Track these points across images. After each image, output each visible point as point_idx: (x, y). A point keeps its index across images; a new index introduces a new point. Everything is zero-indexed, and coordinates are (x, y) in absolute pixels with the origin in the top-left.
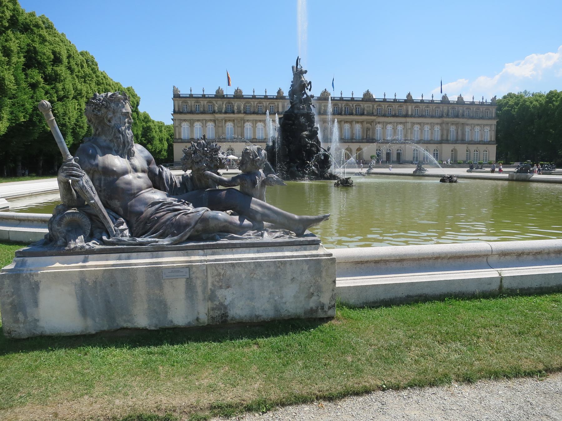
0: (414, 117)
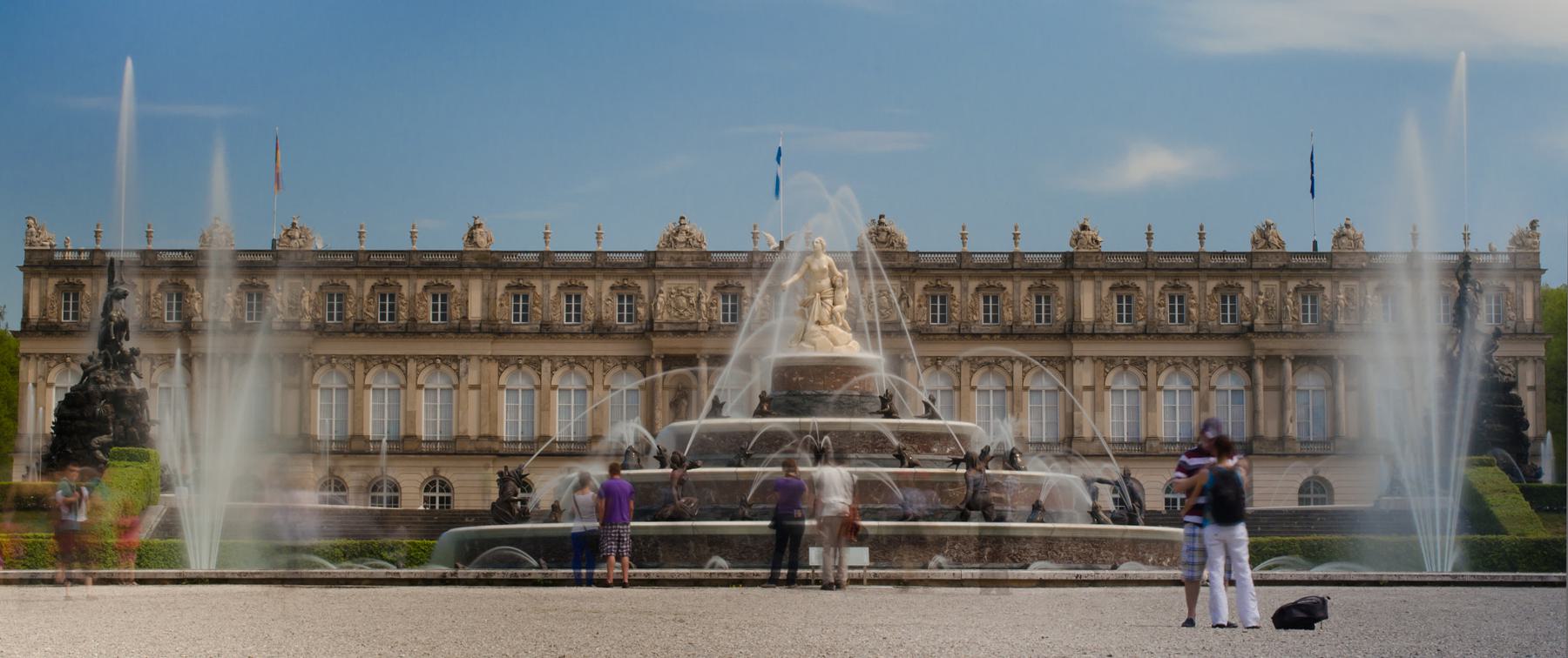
0: (1110, 336)
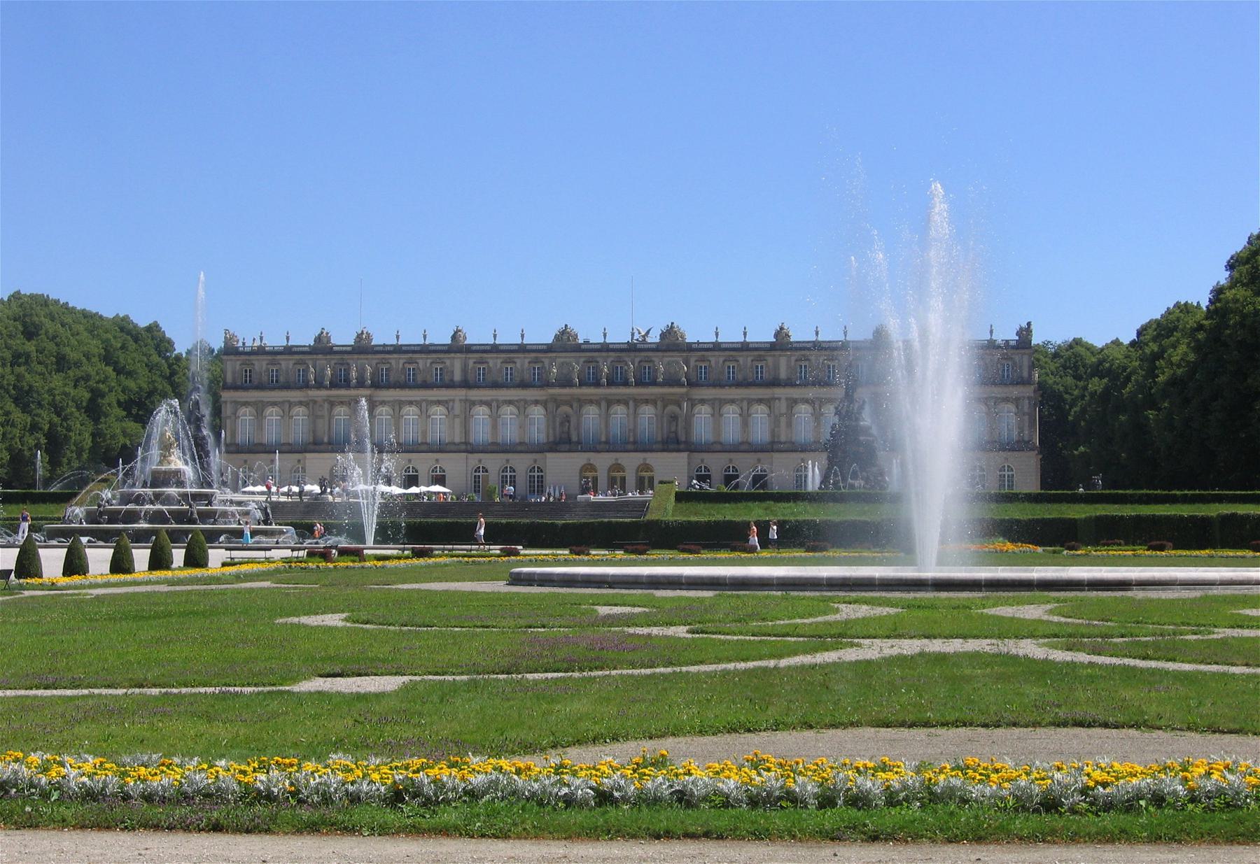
0: (793, 385)
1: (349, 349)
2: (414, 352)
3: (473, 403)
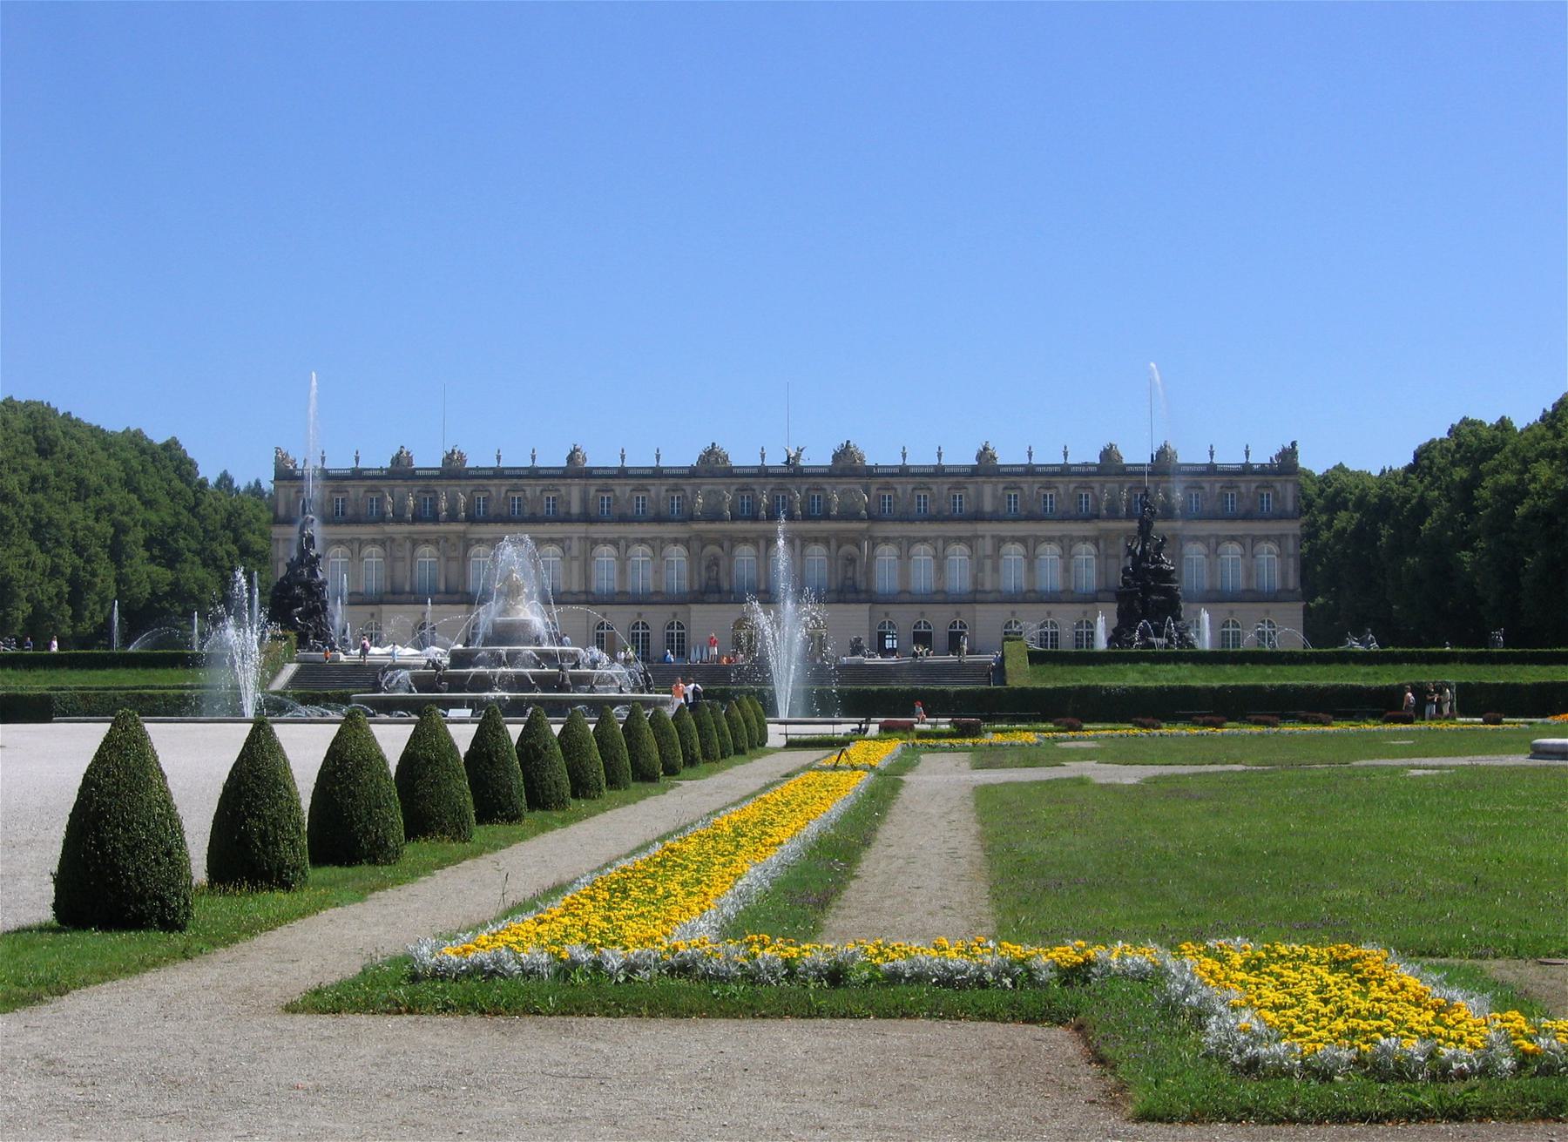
1: (436, 473)
2: (520, 477)
3: (595, 542)
